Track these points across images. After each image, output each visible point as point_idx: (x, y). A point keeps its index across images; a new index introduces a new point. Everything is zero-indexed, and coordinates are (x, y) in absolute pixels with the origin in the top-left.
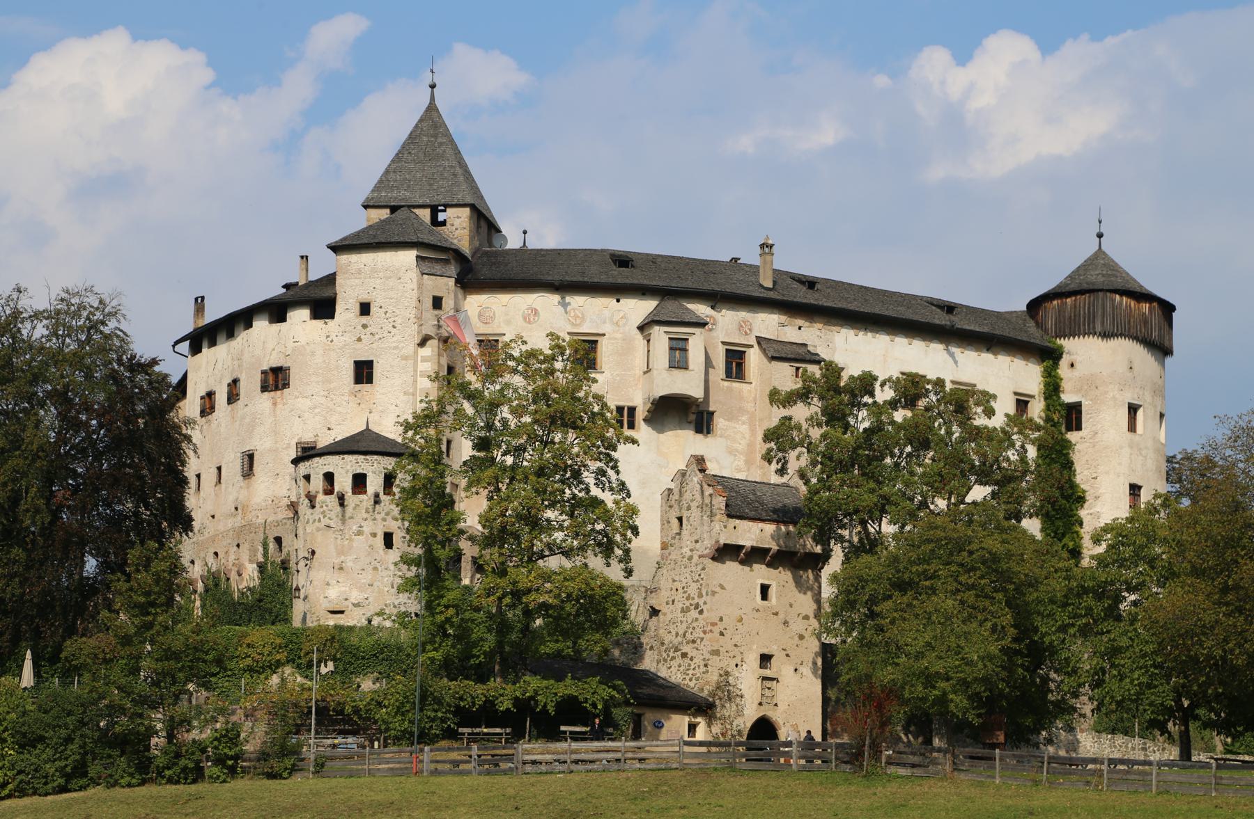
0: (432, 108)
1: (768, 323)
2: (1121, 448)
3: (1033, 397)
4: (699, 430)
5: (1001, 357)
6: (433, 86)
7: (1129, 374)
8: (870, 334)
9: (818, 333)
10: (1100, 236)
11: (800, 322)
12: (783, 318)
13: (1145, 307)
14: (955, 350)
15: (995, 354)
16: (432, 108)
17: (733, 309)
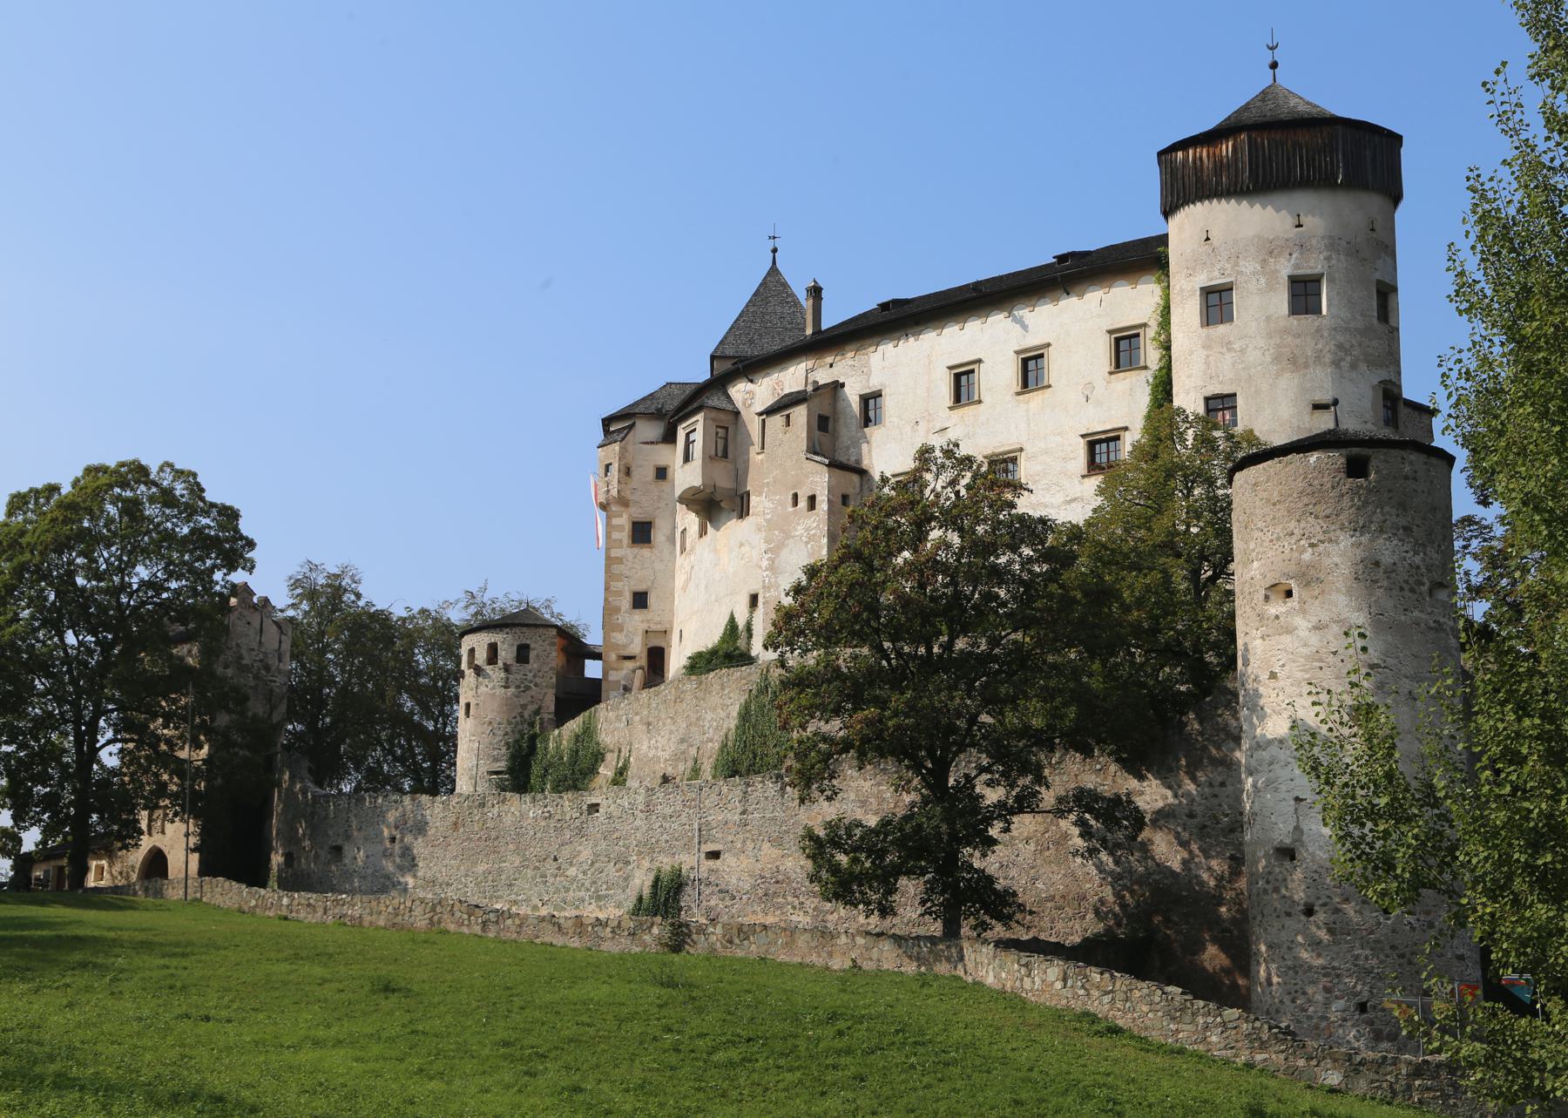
0: (774, 271)
1: (792, 377)
2: (1191, 353)
3: (1145, 325)
4: (741, 517)
5: (1088, 296)
6: (775, 251)
7: (1206, 248)
8: (912, 339)
9: (851, 362)
10: (1274, 66)
11: (829, 360)
12: (810, 364)
13: (1226, 148)
14: (1023, 312)
15: (1081, 296)
16: (774, 271)
17: (768, 375)
